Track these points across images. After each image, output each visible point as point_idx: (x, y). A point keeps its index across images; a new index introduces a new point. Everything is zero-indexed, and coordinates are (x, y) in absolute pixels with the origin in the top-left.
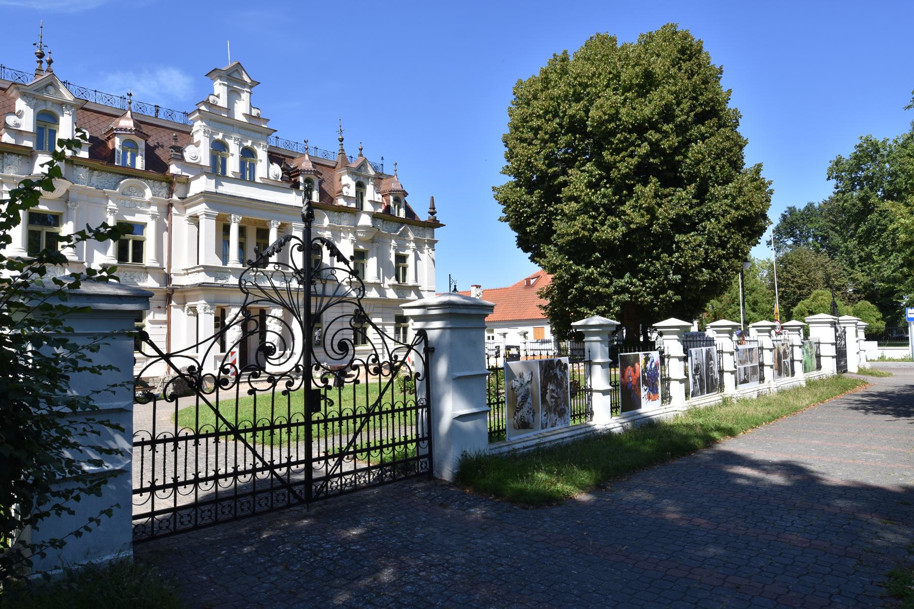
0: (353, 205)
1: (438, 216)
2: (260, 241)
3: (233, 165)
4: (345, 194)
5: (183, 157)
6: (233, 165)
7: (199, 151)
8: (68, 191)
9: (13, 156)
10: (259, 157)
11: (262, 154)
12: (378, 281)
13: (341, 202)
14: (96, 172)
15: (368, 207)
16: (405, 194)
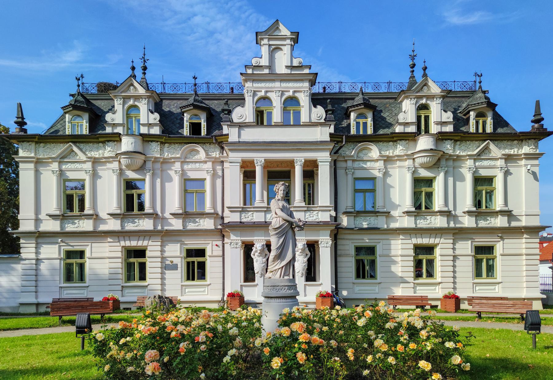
0: (412, 129)
1: (548, 125)
2: (305, 181)
3: (277, 116)
4: (400, 121)
5: (231, 121)
6: (277, 116)
7: (244, 113)
8: (145, 162)
9: (111, 142)
10: (302, 103)
11: (304, 100)
12: (446, 209)
13: (398, 129)
14: (166, 145)
15: (434, 129)
16: (492, 106)
